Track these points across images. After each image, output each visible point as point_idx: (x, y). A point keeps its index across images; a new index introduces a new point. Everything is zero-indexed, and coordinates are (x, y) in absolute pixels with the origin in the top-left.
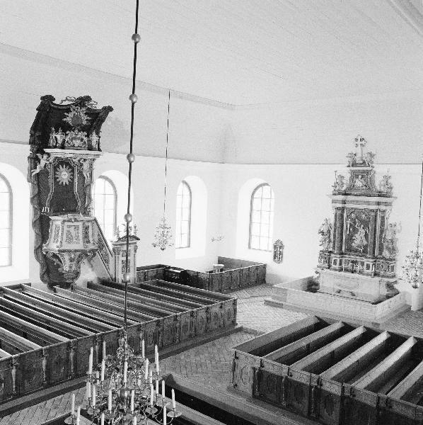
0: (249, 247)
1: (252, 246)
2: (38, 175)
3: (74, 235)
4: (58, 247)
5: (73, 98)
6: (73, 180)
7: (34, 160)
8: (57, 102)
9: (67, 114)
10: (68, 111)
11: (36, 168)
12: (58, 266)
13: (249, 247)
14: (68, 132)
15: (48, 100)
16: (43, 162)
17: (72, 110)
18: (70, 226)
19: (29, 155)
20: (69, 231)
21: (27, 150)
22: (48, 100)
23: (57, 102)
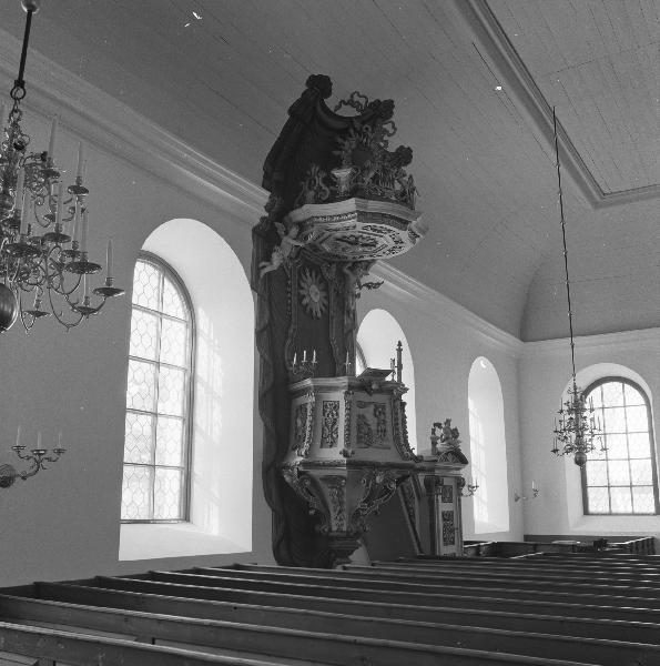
0: (586, 512)
1: (592, 509)
2: (269, 273)
3: (374, 427)
4: (345, 454)
5: (362, 101)
6: (327, 307)
7: (265, 238)
8: (331, 103)
9: (340, 140)
10: (344, 133)
11: (268, 258)
12: (322, 517)
13: (586, 512)
14: (368, 163)
15: (320, 86)
16: (289, 243)
17: (352, 131)
18: (362, 405)
19: (257, 221)
20: (361, 417)
21: (255, 200)
22: (320, 86)
23: (331, 103)
